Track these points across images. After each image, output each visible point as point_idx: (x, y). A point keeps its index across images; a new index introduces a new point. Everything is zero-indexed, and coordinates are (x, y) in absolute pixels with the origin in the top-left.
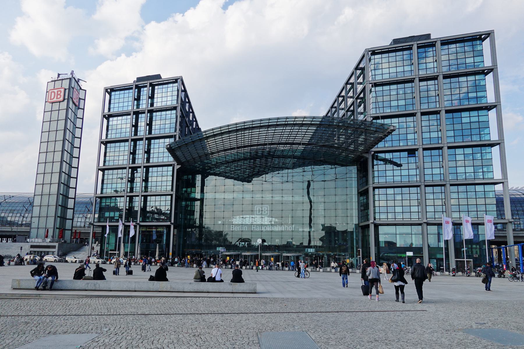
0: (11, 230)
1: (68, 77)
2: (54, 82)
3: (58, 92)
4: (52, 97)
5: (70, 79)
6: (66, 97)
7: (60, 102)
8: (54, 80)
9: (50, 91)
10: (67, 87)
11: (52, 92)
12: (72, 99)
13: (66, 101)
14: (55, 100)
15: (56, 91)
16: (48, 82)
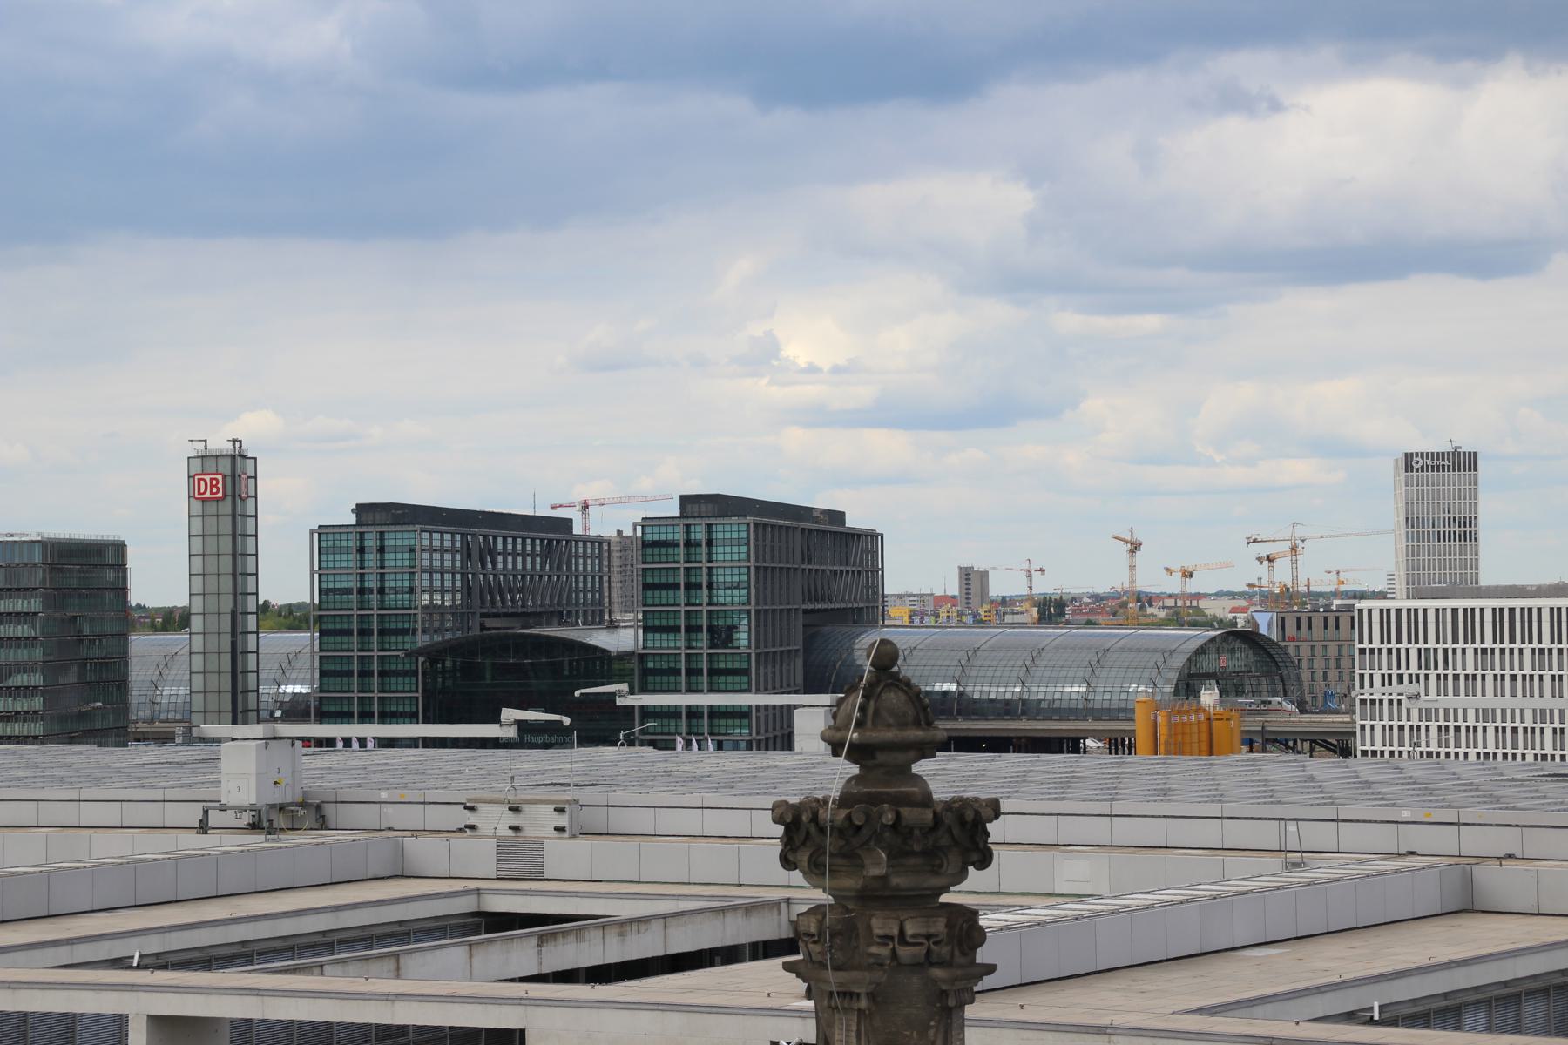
1: (229, 453)
2: (200, 460)
3: (212, 480)
4: (202, 490)
5: (233, 457)
6: (229, 491)
7: (217, 500)
8: (200, 454)
9: (196, 477)
10: (228, 472)
11: (199, 480)
12: (240, 495)
13: (229, 499)
14: (208, 495)
15: (208, 478)
16: (189, 458)
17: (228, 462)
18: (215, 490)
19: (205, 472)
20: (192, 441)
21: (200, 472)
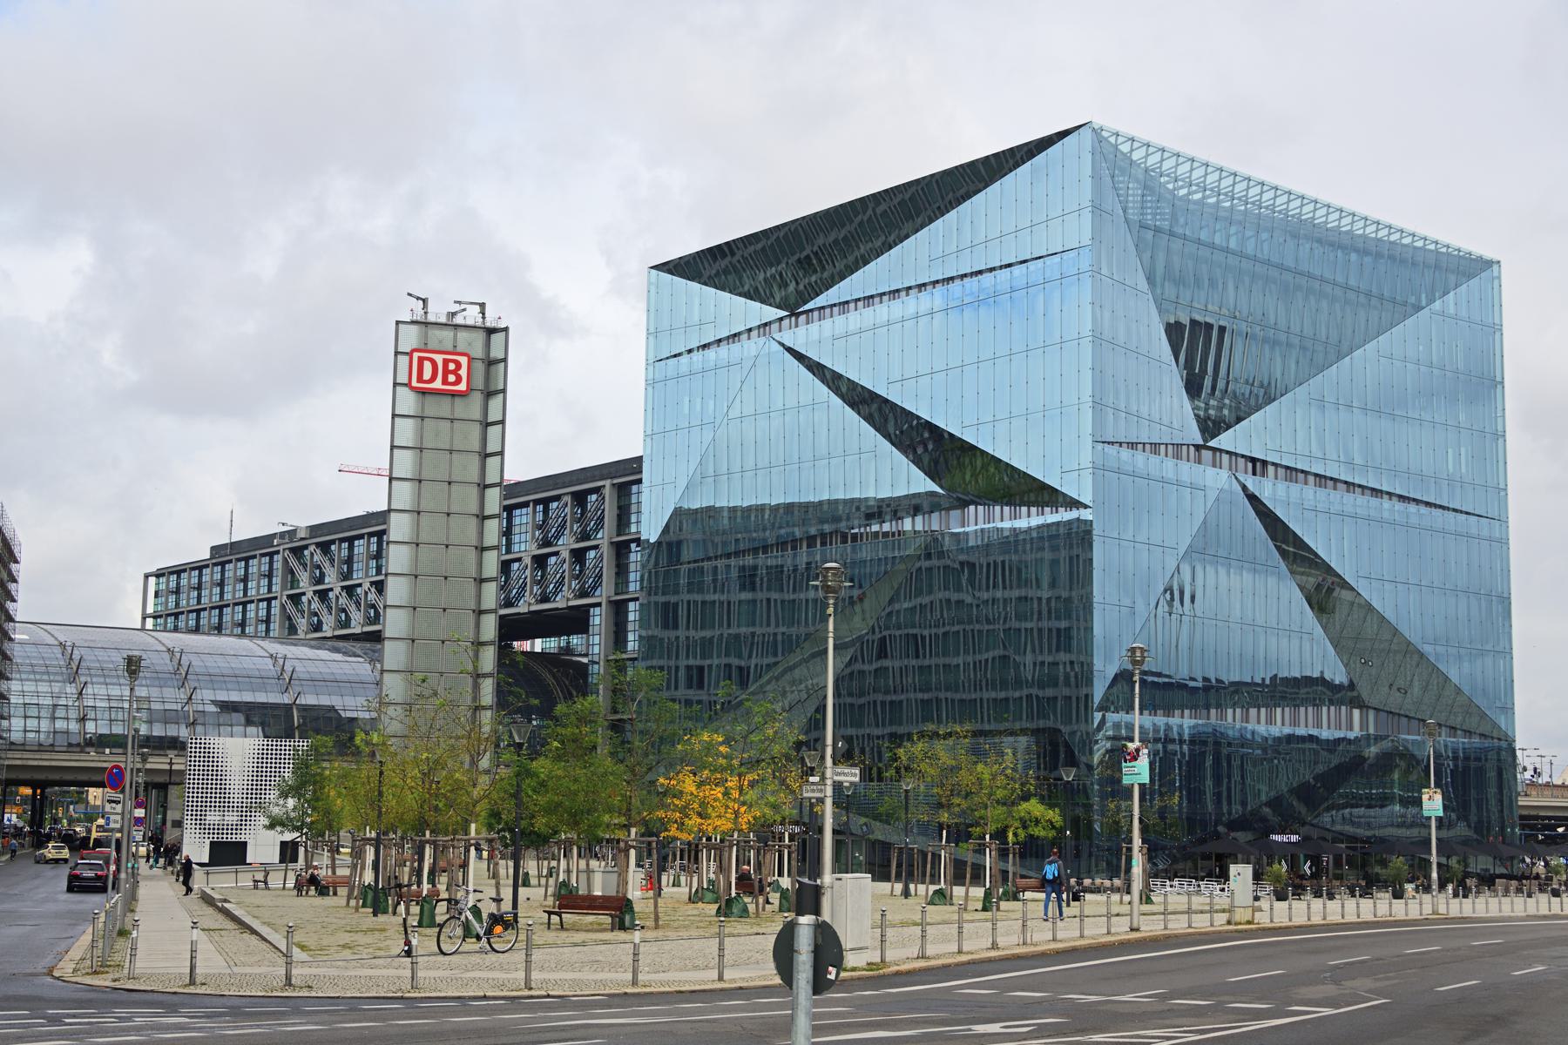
0: (168, 767)
2: (414, 328)
3: (446, 362)
4: (427, 375)
6: (479, 382)
7: (454, 394)
9: (416, 355)
10: (478, 352)
11: (421, 360)
13: (477, 398)
14: (438, 384)
15: (439, 359)
16: (398, 323)
17: (480, 337)
18: (452, 378)
19: (430, 347)
20: (410, 295)
21: (415, 347)
